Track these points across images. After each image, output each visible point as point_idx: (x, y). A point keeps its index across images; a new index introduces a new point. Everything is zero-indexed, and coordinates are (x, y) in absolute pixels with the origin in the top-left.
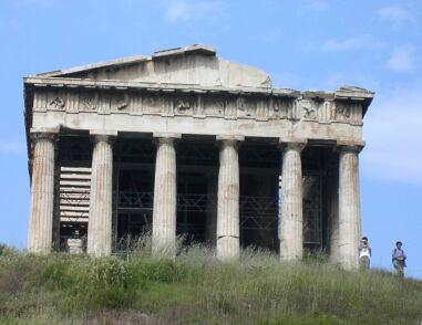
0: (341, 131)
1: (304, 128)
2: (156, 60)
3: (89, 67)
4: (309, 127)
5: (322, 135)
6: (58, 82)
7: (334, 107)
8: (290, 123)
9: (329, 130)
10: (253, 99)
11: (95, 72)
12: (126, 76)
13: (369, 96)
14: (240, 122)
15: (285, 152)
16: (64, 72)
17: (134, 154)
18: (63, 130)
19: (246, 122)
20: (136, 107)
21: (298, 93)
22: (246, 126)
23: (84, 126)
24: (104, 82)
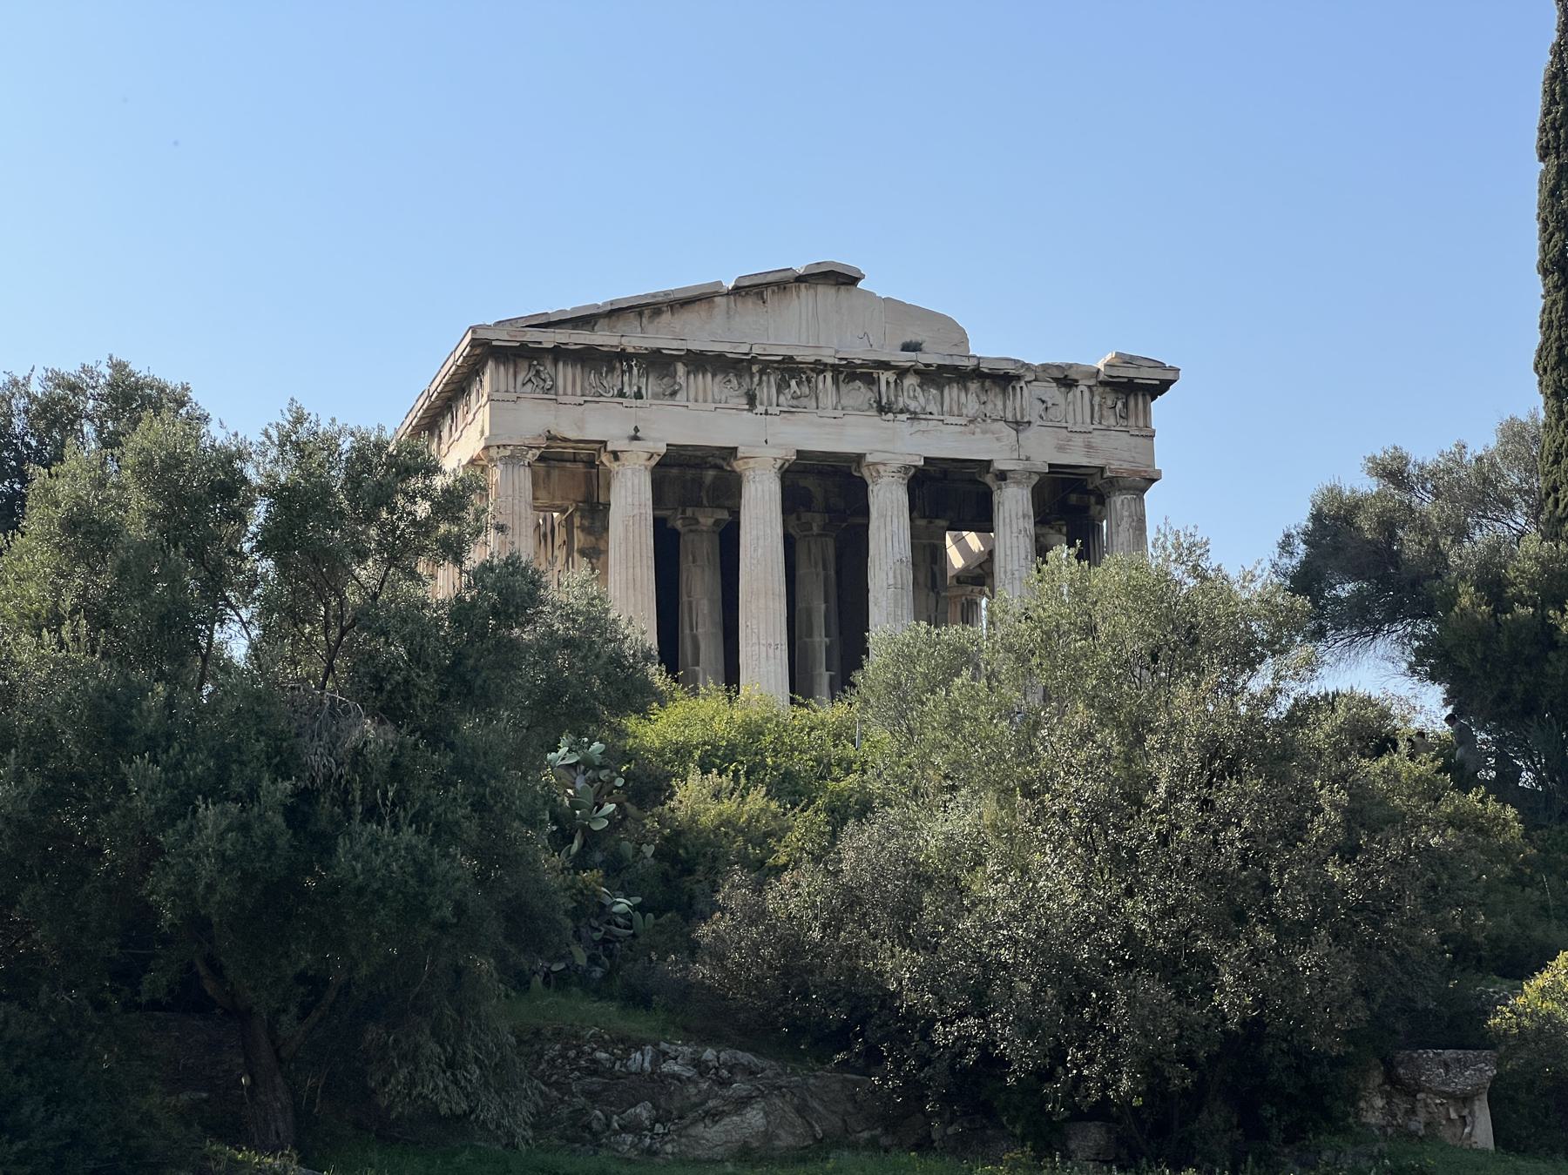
5: (1075, 457)
7: (1097, 399)
9: (1089, 446)
13: (1170, 376)
17: (695, 488)
21: (1027, 367)
24: (636, 338)
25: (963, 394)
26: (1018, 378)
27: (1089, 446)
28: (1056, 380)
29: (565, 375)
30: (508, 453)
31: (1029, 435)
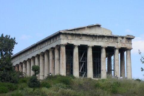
0: (127, 46)
1: (120, 44)
2: (88, 27)
4: (121, 44)
5: (123, 46)
6: (67, 32)
8: (117, 43)
9: (125, 45)
10: (109, 37)
11: (74, 30)
12: (81, 30)
14: (106, 43)
15: (115, 50)
18: (68, 44)
19: (107, 43)
20: (84, 38)
22: (108, 44)
23: (72, 43)
27: (125, 45)
31: (119, 43)
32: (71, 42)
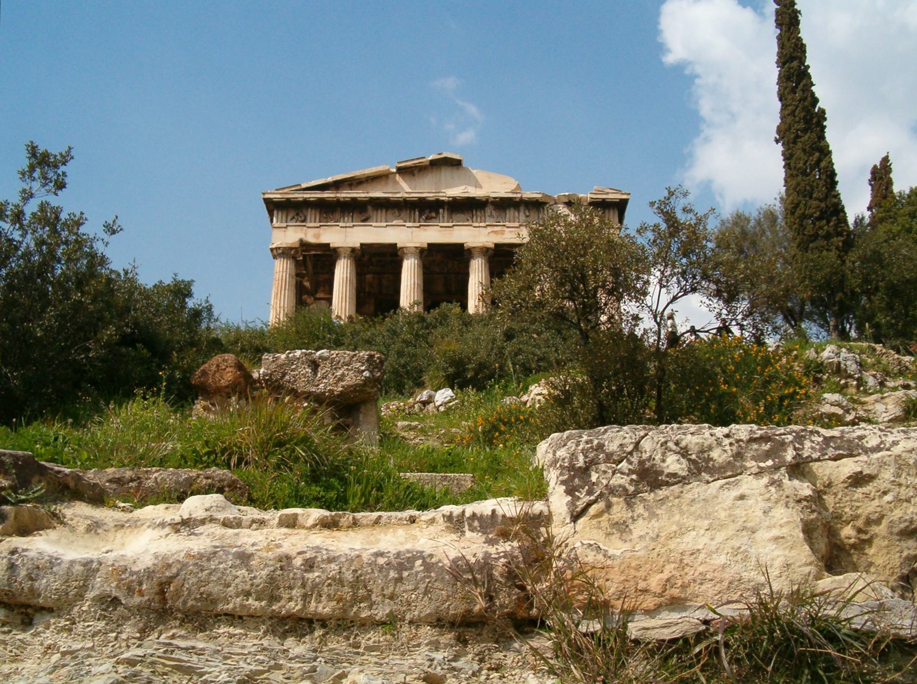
3: (330, 179)
6: (296, 196)
11: (337, 185)
13: (624, 197)
16: (304, 186)
18: (304, 245)
19: (496, 229)
23: (324, 240)
24: (345, 194)
25: (517, 214)
26: (545, 203)
28: (565, 203)
29: (310, 214)
30: (280, 251)
32: (317, 236)
